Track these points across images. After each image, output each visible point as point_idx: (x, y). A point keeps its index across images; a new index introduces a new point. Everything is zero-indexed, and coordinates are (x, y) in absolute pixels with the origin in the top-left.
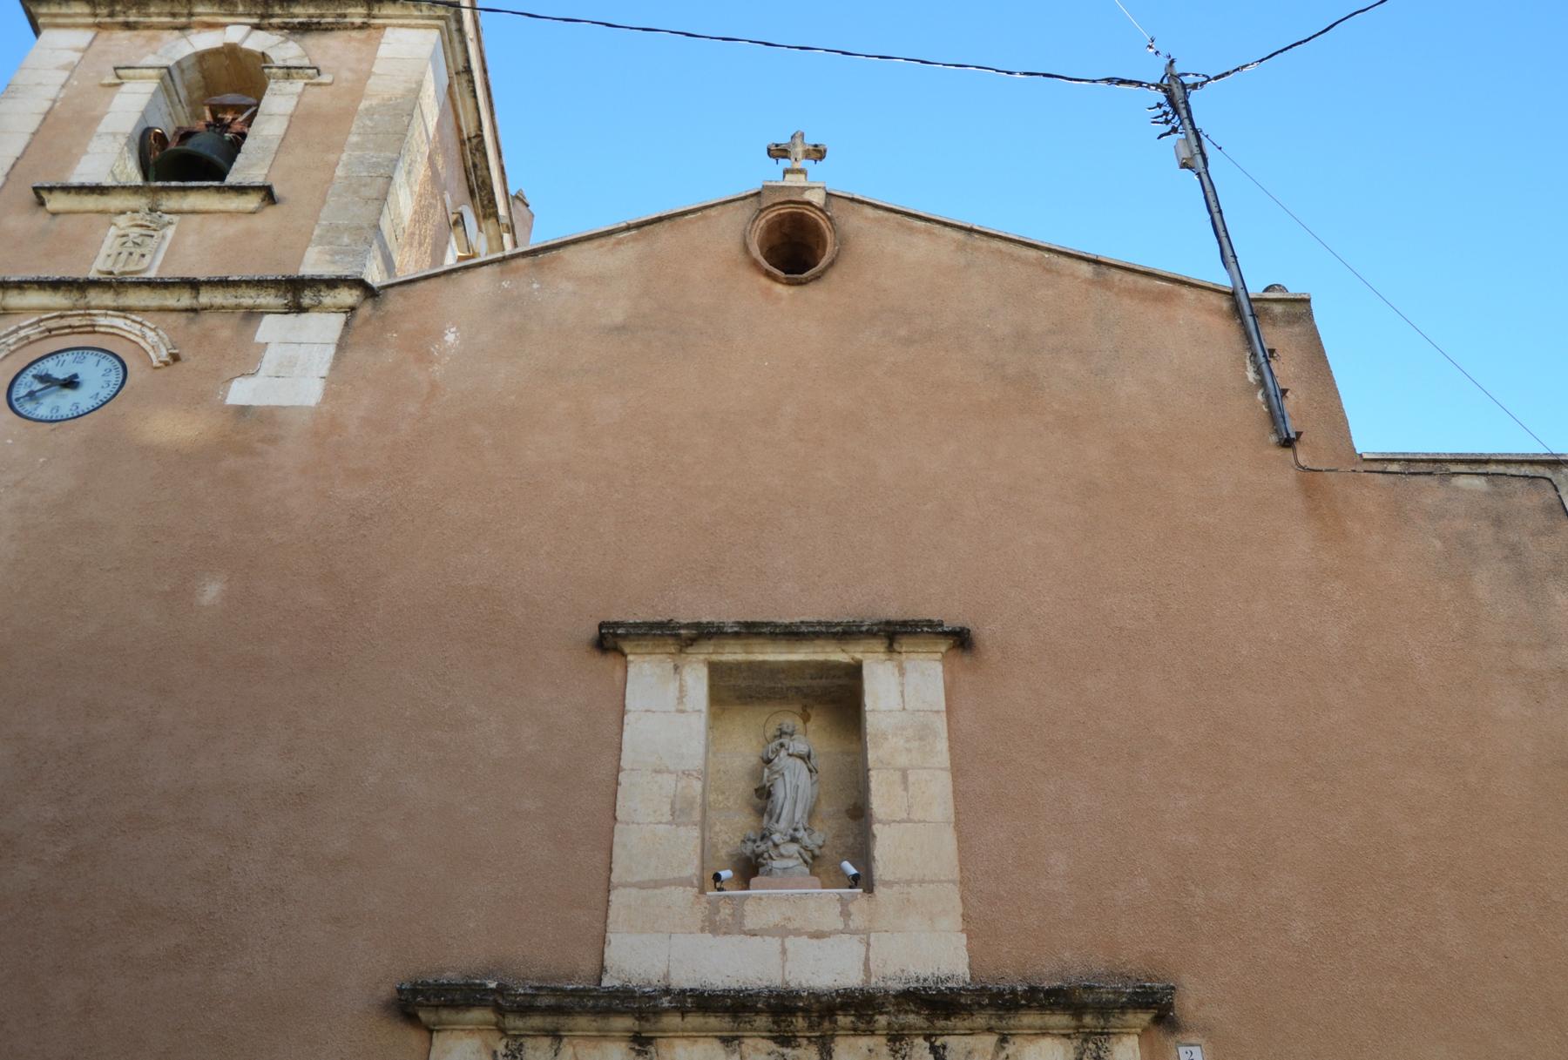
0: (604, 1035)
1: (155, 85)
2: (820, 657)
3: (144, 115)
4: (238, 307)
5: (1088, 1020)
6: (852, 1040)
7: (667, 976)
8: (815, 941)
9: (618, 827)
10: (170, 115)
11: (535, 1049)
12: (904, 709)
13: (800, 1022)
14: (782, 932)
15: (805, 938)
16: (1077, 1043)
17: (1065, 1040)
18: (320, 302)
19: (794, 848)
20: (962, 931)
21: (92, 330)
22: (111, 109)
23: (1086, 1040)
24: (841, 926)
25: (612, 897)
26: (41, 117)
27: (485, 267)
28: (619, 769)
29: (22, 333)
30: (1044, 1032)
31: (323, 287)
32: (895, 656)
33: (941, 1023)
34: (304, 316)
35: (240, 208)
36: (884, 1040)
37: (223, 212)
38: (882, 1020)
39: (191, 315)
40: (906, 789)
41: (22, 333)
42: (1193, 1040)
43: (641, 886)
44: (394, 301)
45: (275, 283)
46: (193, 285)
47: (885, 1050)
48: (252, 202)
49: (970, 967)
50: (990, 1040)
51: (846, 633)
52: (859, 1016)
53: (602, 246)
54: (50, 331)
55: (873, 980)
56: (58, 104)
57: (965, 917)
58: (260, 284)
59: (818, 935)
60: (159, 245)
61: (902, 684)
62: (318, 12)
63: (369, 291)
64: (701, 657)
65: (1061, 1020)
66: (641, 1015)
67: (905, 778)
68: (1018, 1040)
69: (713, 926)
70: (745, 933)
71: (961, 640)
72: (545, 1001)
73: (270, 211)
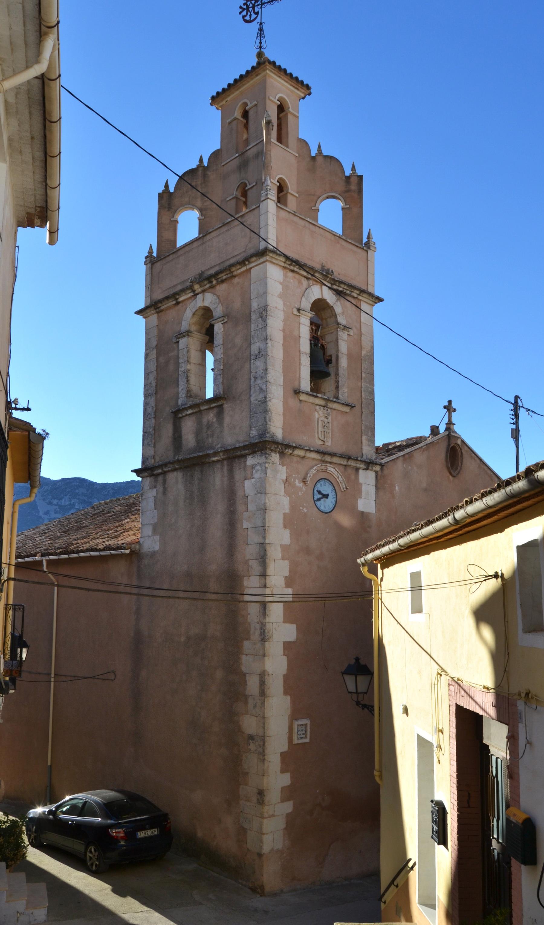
35: (345, 411)
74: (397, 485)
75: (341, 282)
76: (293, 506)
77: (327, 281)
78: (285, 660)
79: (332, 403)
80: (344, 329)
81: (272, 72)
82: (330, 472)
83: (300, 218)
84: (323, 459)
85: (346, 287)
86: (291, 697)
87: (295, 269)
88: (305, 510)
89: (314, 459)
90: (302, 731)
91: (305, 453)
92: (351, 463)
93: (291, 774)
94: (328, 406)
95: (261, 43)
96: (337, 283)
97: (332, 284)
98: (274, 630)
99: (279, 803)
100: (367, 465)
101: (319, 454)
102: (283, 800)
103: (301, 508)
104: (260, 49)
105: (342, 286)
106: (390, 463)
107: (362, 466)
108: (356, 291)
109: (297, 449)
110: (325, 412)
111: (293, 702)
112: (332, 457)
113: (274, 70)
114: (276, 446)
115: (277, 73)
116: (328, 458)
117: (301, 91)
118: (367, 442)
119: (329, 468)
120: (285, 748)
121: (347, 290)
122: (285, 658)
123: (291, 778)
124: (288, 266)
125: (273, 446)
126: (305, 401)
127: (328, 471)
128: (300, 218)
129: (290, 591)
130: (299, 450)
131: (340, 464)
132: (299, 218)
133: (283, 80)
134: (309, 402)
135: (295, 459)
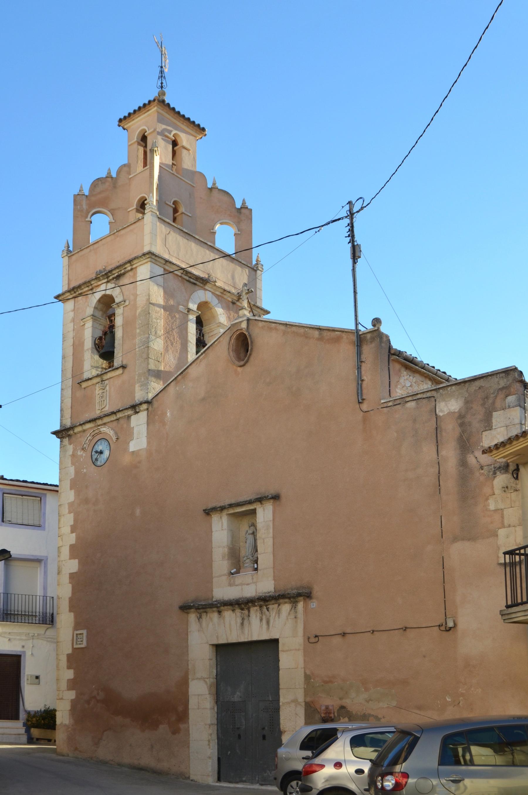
0: (213, 612)
1: (91, 322)
2: (248, 509)
3: (92, 337)
4: (125, 416)
5: (292, 600)
6: (253, 608)
7: (223, 597)
8: (247, 586)
9: (213, 563)
10: (100, 324)
11: (204, 615)
12: (264, 521)
13: (243, 606)
14: (242, 584)
15: (246, 586)
16: (292, 604)
17: (290, 604)
18: (140, 410)
19: (248, 561)
20: (273, 580)
21: (100, 433)
22: (85, 338)
23: (293, 604)
24: (252, 582)
25: (213, 580)
26: (72, 347)
27: (172, 383)
28: (212, 548)
29: (89, 439)
30: (286, 603)
31: (139, 405)
32: (263, 505)
33: (267, 603)
34: (139, 414)
36: (258, 607)
37: (116, 376)
38: (256, 604)
39: (117, 421)
40: (264, 544)
41: (89, 439)
42: (314, 601)
43: (218, 577)
44: (156, 404)
45: (129, 408)
46: (113, 413)
47: (259, 609)
48: (120, 371)
49: (274, 588)
50: (277, 605)
51: (250, 502)
52: (252, 603)
53: (197, 364)
54: (93, 436)
55: (257, 594)
56: (74, 338)
57: (274, 576)
58: (126, 409)
59: (248, 584)
60: (106, 394)
61: (264, 514)
62: (119, 270)
63: (148, 402)
64: (225, 513)
65: (287, 600)
66: (218, 607)
67: (264, 541)
68: (281, 605)
69: (230, 585)
70: (235, 586)
71: (276, 498)
72: (200, 607)
73: (126, 371)
74: (169, 411)
75: (110, 271)
76: (77, 472)
77: (102, 280)
78: (70, 586)
79: (105, 375)
80: (118, 306)
81: (127, 124)
82: (104, 432)
83: (86, 248)
84: (96, 425)
85: (117, 271)
86: (74, 614)
87: (80, 292)
88: (85, 471)
89: (91, 428)
90: (81, 639)
91: (82, 428)
92: (119, 415)
93: (74, 671)
94: (104, 379)
95: (162, 83)
96: (109, 274)
97: (108, 278)
98: (63, 565)
99: (66, 690)
100: (134, 409)
101: (92, 423)
102: (69, 688)
103: (82, 470)
104: (162, 89)
105: (114, 272)
106: (160, 395)
107: (130, 412)
108: (126, 266)
109: (75, 428)
110: (100, 386)
111: (76, 617)
112: (102, 420)
113: (127, 121)
114: (62, 434)
115: (129, 121)
116: (99, 422)
117: (153, 108)
118: (140, 388)
119: (101, 429)
120: (70, 651)
121: (121, 271)
122: (70, 585)
123: (74, 673)
124: (75, 295)
125: (60, 435)
126: (87, 387)
127: (102, 432)
128: (86, 248)
129: (74, 535)
130: (77, 428)
131: (112, 421)
132: (85, 249)
133: (137, 118)
134: (91, 385)
135: (79, 435)
